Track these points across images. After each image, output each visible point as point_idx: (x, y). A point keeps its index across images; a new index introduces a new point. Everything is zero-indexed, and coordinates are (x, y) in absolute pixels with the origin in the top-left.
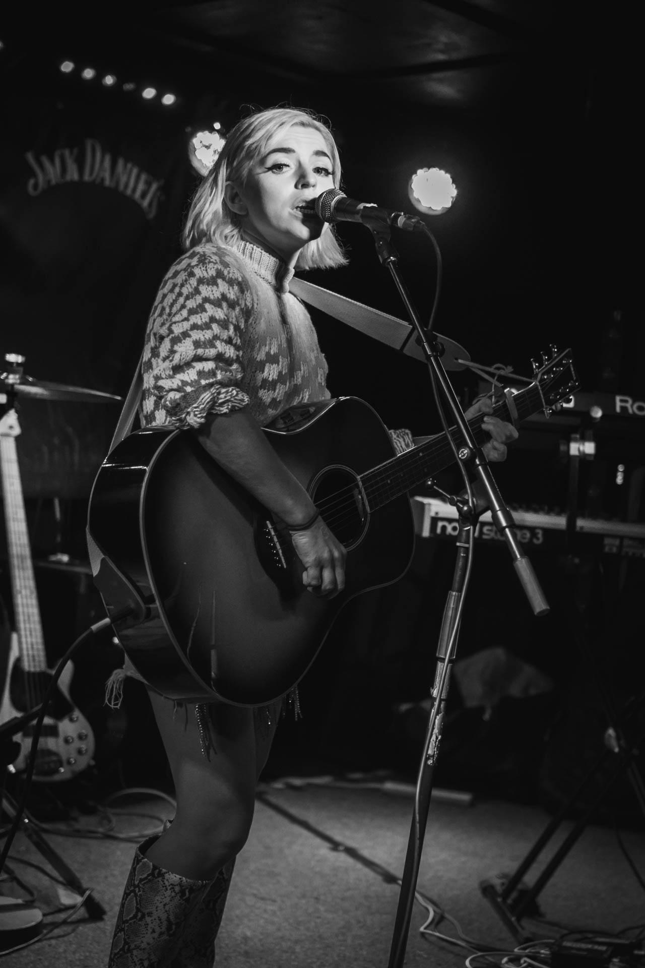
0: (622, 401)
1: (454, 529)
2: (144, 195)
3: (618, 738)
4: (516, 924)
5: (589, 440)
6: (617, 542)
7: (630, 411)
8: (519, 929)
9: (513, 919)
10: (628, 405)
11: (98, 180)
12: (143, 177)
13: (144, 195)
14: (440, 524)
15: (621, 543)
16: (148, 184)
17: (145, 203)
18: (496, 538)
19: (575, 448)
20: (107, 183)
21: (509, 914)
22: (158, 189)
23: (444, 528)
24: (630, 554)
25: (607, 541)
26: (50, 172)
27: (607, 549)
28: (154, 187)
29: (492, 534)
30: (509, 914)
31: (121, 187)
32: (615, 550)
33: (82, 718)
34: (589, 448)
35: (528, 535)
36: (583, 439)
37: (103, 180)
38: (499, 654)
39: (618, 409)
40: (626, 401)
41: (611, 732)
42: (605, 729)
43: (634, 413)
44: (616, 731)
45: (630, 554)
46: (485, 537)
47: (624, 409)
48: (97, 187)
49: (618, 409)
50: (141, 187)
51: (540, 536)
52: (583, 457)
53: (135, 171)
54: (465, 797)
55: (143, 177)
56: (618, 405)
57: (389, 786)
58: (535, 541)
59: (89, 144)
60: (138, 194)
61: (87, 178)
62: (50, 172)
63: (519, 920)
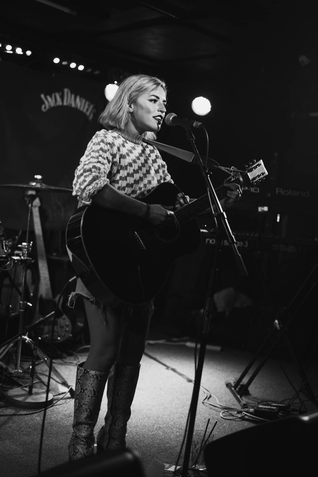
0: (278, 190)
1: (213, 241)
2: (87, 110)
3: (279, 324)
4: (240, 398)
5: (266, 206)
7: (282, 193)
8: (241, 400)
9: (239, 396)
10: (281, 191)
14: (207, 240)
16: (89, 106)
19: (260, 209)
20: (73, 105)
21: (237, 395)
22: (93, 108)
23: (209, 241)
26: (50, 102)
28: (91, 107)
30: (237, 395)
33: (66, 318)
34: (266, 209)
35: (242, 244)
37: (71, 104)
38: (231, 289)
39: (277, 193)
41: (276, 321)
42: (275, 320)
44: (278, 321)
46: (225, 245)
47: (279, 193)
48: (69, 108)
49: (277, 193)
50: (86, 107)
51: (247, 244)
52: (263, 212)
54: (218, 348)
55: (87, 103)
56: (277, 191)
57: (189, 344)
58: (245, 246)
59: (66, 90)
60: (85, 110)
61: (65, 104)
62: (50, 102)
63: (241, 397)
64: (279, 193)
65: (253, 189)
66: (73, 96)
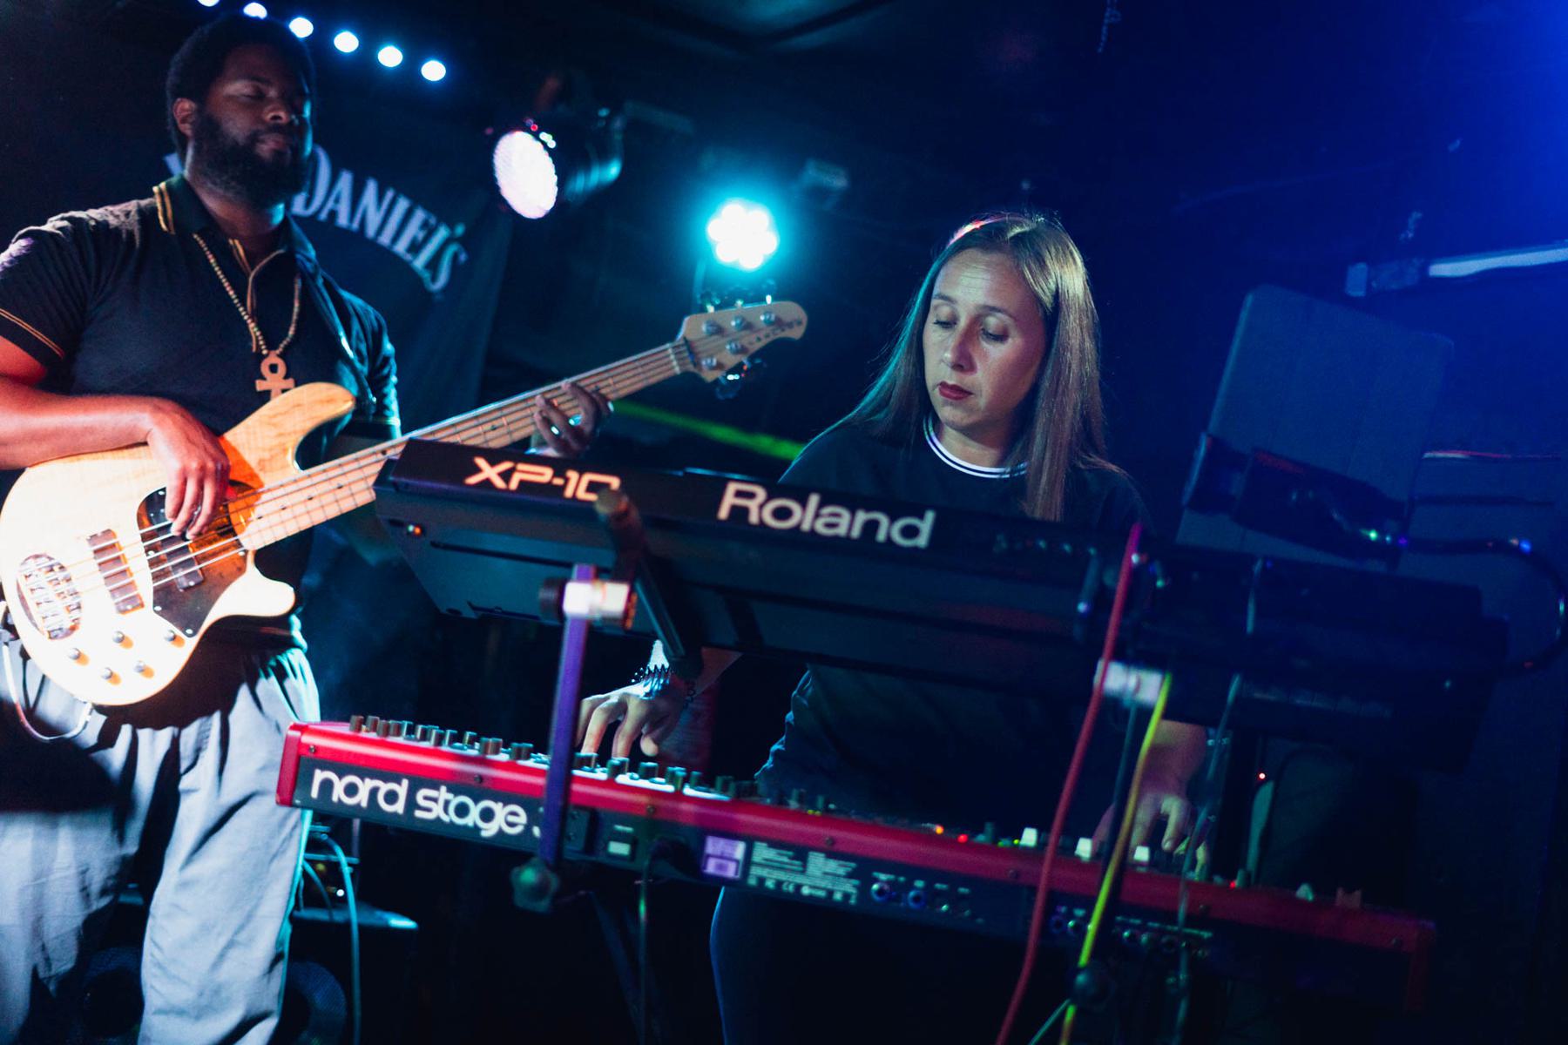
2: (415, 248)
6: (739, 850)
7: (754, 518)
10: (753, 505)
11: (323, 216)
12: (420, 215)
13: (415, 248)
14: (319, 776)
15: (749, 853)
17: (419, 263)
18: (445, 818)
20: (343, 220)
23: (327, 786)
24: (770, 884)
25: (713, 845)
27: (711, 867)
28: (442, 233)
29: (437, 811)
31: (371, 231)
32: (731, 872)
35: (523, 818)
36: (602, 574)
37: (333, 214)
39: (723, 513)
40: (751, 496)
43: (762, 524)
45: (770, 884)
46: (419, 814)
47: (739, 513)
49: (723, 513)
50: (413, 230)
53: (403, 205)
56: (729, 500)
60: (401, 247)
64: (739, 513)
65: (588, 477)
66: (345, 181)
